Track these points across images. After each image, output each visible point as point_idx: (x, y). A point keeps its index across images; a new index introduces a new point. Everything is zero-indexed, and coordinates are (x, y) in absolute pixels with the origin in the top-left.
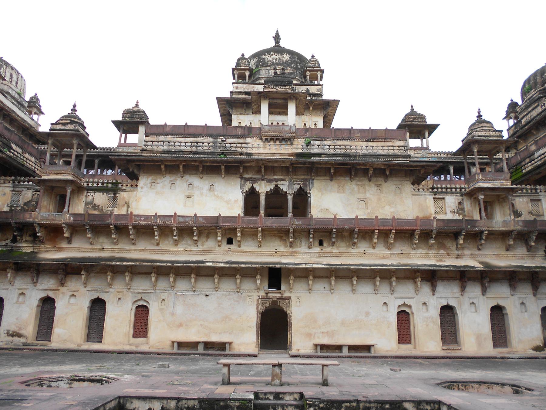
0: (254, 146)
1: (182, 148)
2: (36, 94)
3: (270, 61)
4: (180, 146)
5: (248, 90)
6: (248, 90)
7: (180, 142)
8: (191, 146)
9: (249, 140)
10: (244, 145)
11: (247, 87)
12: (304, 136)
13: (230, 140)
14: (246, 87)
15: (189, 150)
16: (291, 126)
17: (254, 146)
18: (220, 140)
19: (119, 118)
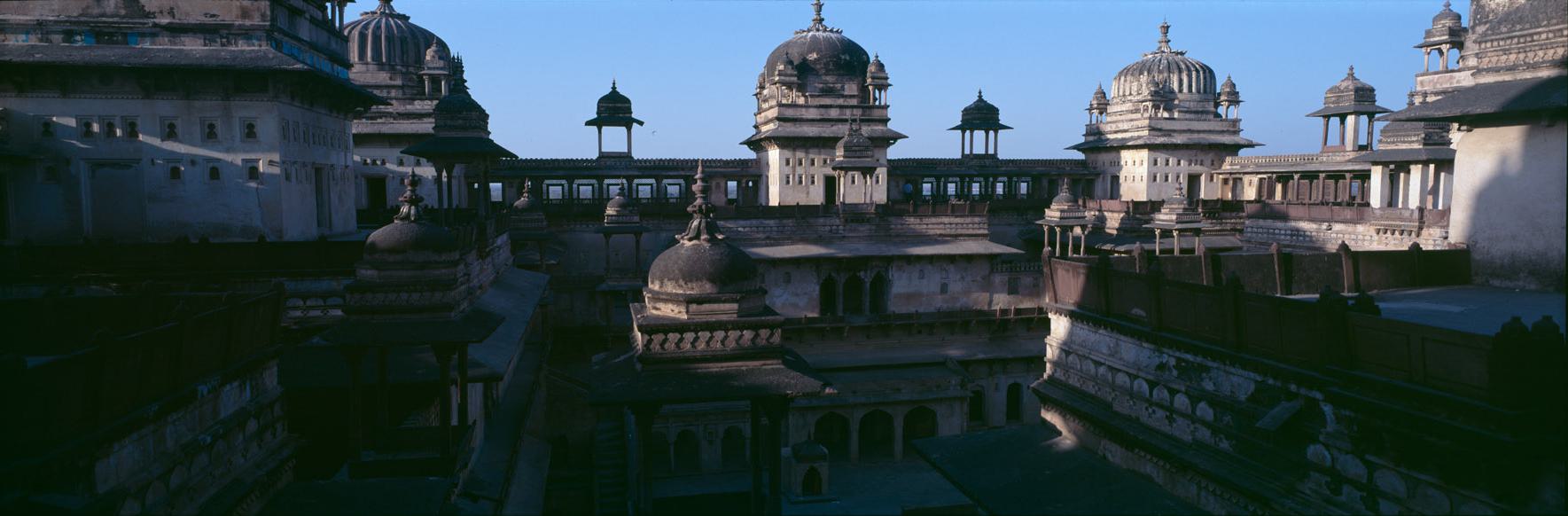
0: (1366, 238)
1: (1283, 237)
2: (1229, 77)
3: (1493, 11)
4: (1280, 234)
5: (1441, 85)
6: (1441, 85)
7: (1280, 230)
8: (1292, 235)
9: (1360, 228)
10: (1353, 236)
11: (1440, 80)
12: (1440, 224)
13: (1337, 227)
14: (1438, 79)
15: (1288, 243)
16: (1412, 210)
17: (1366, 238)
18: (1325, 226)
19: (1320, 106)
